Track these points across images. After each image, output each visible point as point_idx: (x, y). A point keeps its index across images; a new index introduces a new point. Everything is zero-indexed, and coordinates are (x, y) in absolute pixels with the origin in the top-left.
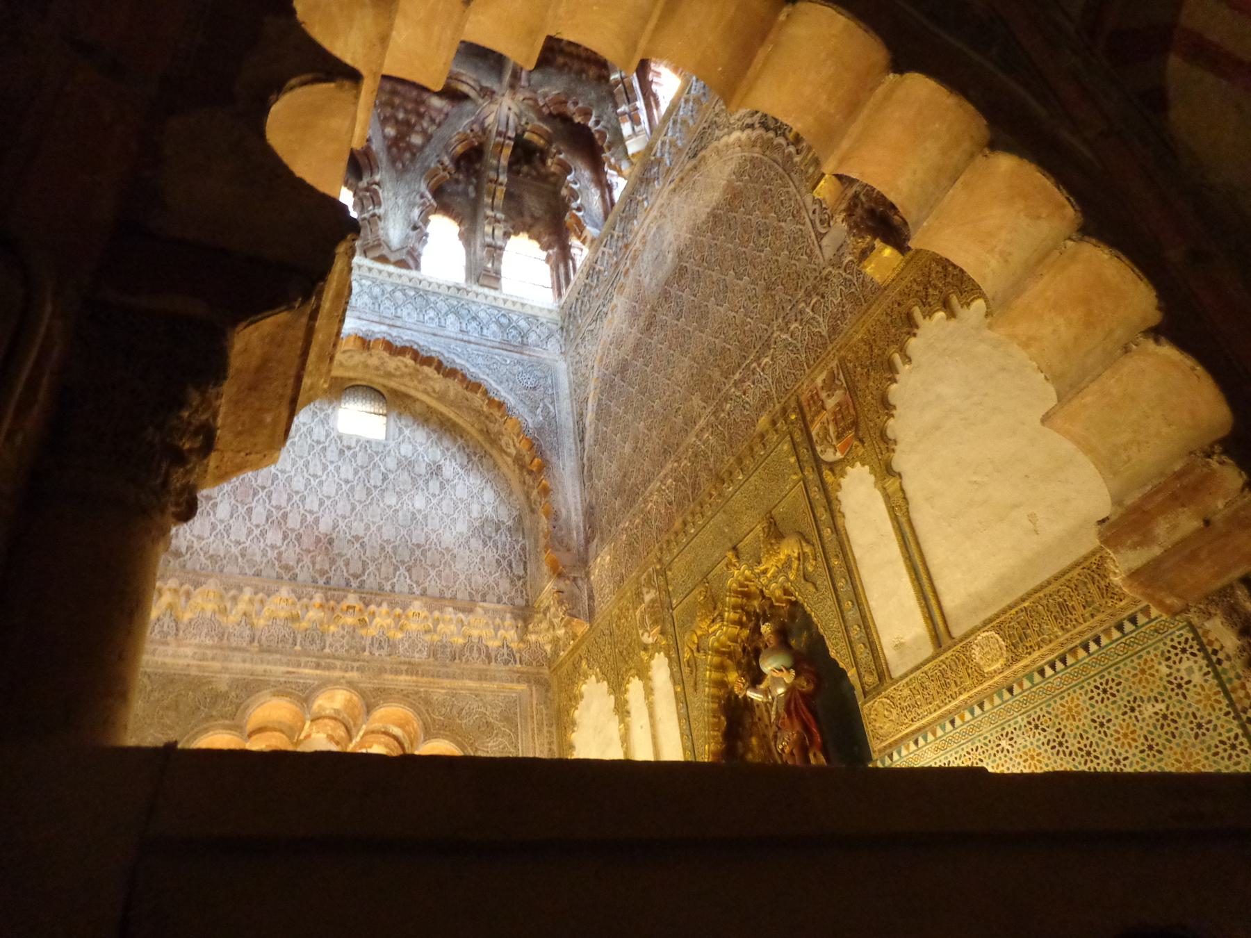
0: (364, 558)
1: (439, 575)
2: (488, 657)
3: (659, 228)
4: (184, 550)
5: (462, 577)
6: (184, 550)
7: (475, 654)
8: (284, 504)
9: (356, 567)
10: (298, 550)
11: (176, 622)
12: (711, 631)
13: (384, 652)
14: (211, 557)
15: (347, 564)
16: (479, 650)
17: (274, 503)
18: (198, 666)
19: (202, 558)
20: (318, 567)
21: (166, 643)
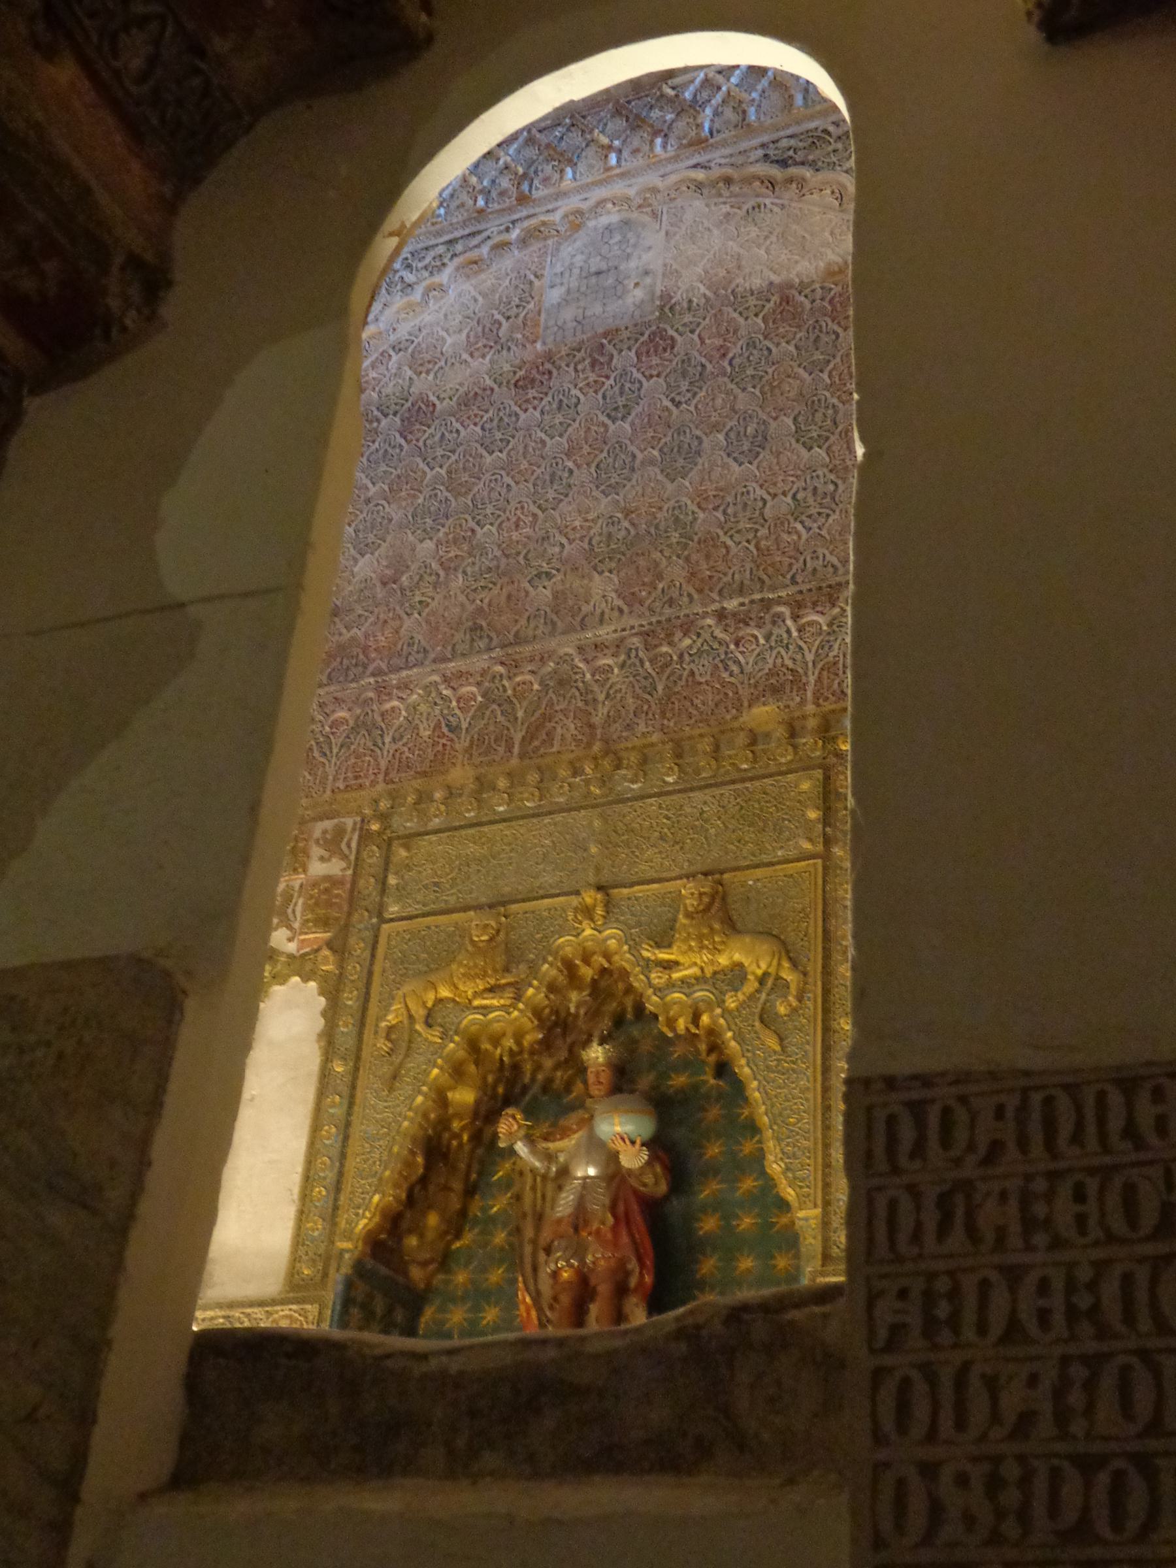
3: (626, 223)
12: (476, 1003)
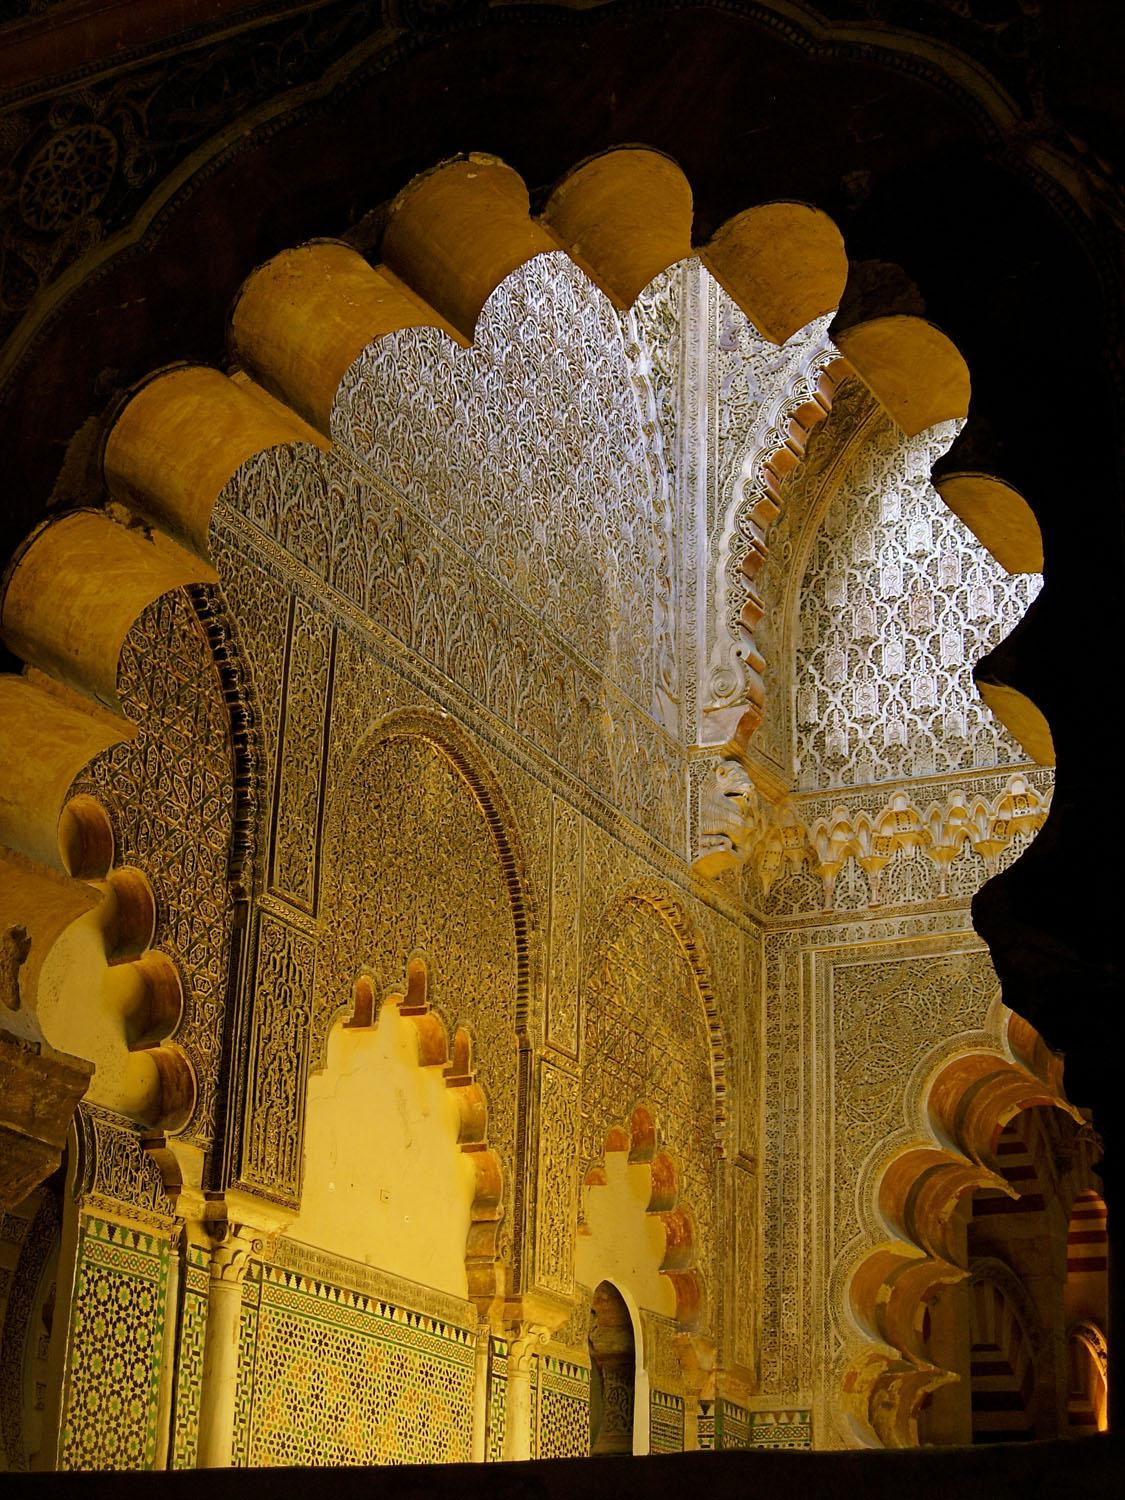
4: (845, 752)
6: (845, 752)
8: (989, 610)
11: (864, 875)
14: (889, 752)
17: (972, 616)
18: (913, 945)
19: (875, 757)
21: (858, 918)
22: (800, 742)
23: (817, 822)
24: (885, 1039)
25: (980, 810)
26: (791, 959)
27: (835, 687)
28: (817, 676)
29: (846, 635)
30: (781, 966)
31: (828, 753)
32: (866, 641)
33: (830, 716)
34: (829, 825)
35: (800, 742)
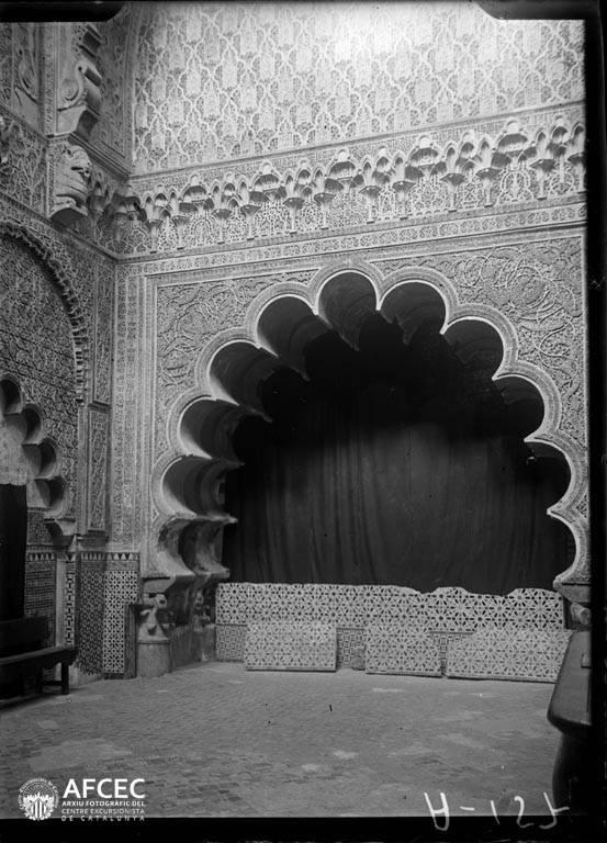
0: (352, 92)
1: (453, 85)
2: (534, 186)
4: (163, 147)
5: (487, 77)
7: (515, 187)
9: (344, 108)
10: (275, 107)
13: (391, 214)
15: (332, 106)
16: (521, 179)
19: (181, 150)
20: (299, 123)
21: (169, 256)
22: (137, 141)
23: (145, 193)
24: (187, 332)
25: (243, 185)
26: (131, 280)
27: (158, 104)
28: (148, 96)
29: (165, 67)
30: (127, 286)
31: (153, 147)
32: (178, 71)
33: (155, 123)
34: (152, 194)
35: (137, 141)
